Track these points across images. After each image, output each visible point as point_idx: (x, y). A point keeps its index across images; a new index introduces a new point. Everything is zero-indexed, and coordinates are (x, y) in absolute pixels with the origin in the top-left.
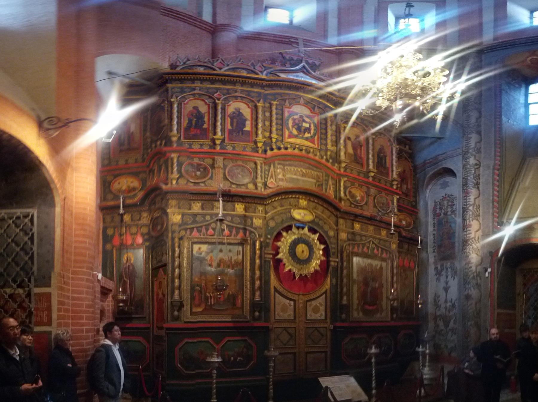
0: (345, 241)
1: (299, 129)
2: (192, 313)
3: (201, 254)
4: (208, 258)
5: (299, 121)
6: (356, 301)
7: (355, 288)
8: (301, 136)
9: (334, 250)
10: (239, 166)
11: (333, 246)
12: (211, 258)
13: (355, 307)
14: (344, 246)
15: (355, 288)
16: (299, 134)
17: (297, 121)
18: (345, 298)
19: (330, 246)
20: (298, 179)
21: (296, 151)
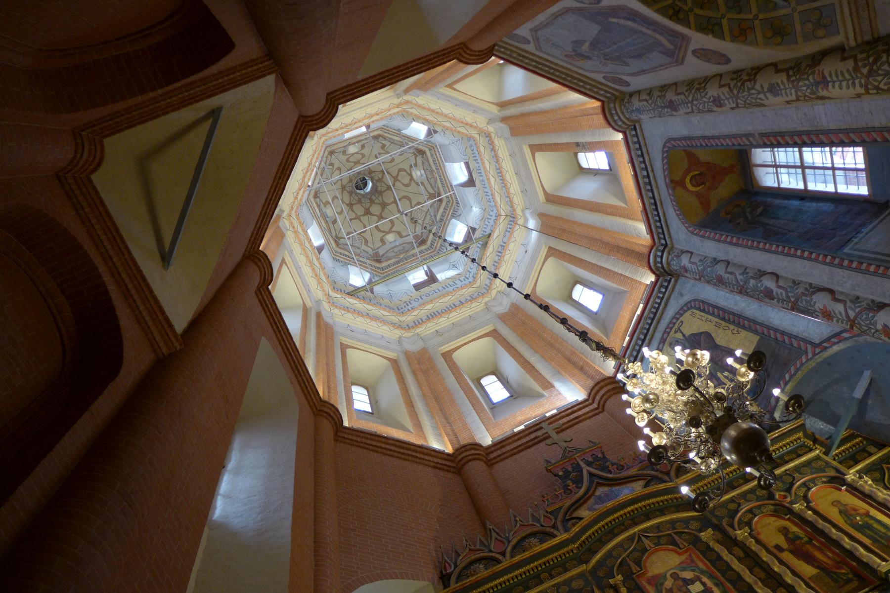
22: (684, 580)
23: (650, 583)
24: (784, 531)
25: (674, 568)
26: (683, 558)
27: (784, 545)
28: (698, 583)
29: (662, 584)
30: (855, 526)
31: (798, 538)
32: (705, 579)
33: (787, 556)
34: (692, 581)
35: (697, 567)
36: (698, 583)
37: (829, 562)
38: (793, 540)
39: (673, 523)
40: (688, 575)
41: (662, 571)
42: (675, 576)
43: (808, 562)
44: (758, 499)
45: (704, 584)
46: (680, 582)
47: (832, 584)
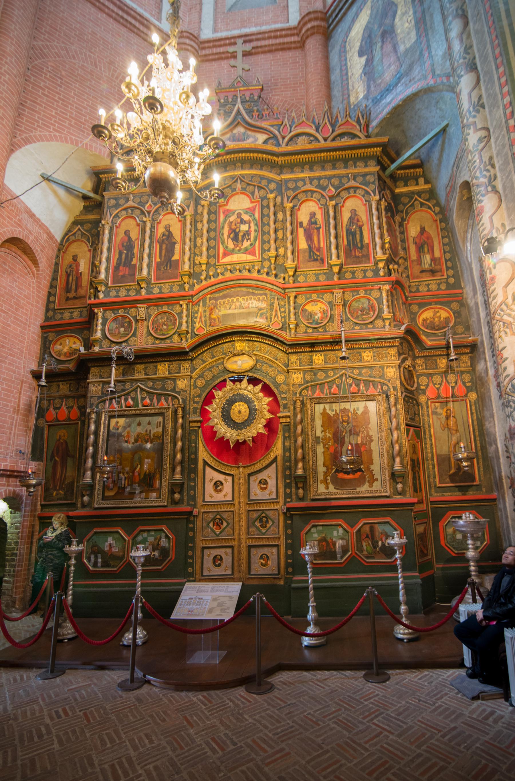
0: (300, 385)
1: (235, 239)
2: (104, 498)
3: (118, 429)
4: (125, 434)
5: (236, 225)
6: (321, 469)
7: (320, 449)
8: (238, 248)
9: (285, 402)
10: (165, 312)
11: (283, 396)
12: (128, 433)
13: (321, 477)
14: (298, 392)
15: (320, 449)
16: (236, 246)
17: (233, 227)
18: (300, 465)
19: (278, 396)
20: (233, 314)
21: (228, 275)
22: (242, 220)
23: (223, 213)
24: (313, 215)
25: (243, 210)
26: (252, 205)
27: (305, 224)
28: (247, 225)
29: (230, 217)
30: (348, 231)
31: (315, 223)
32: (252, 225)
33: (301, 231)
34: (245, 222)
35: (254, 215)
36: (247, 225)
37: (317, 245)
38: (312, 222)
39: (262, 178)
40: (246, 217)
41: (235, 208)
42: (239, 215)
43: (307, 240)
44: (319, 186)
45: (250, 227)
46: (239, 220)
47: (307, 258)
